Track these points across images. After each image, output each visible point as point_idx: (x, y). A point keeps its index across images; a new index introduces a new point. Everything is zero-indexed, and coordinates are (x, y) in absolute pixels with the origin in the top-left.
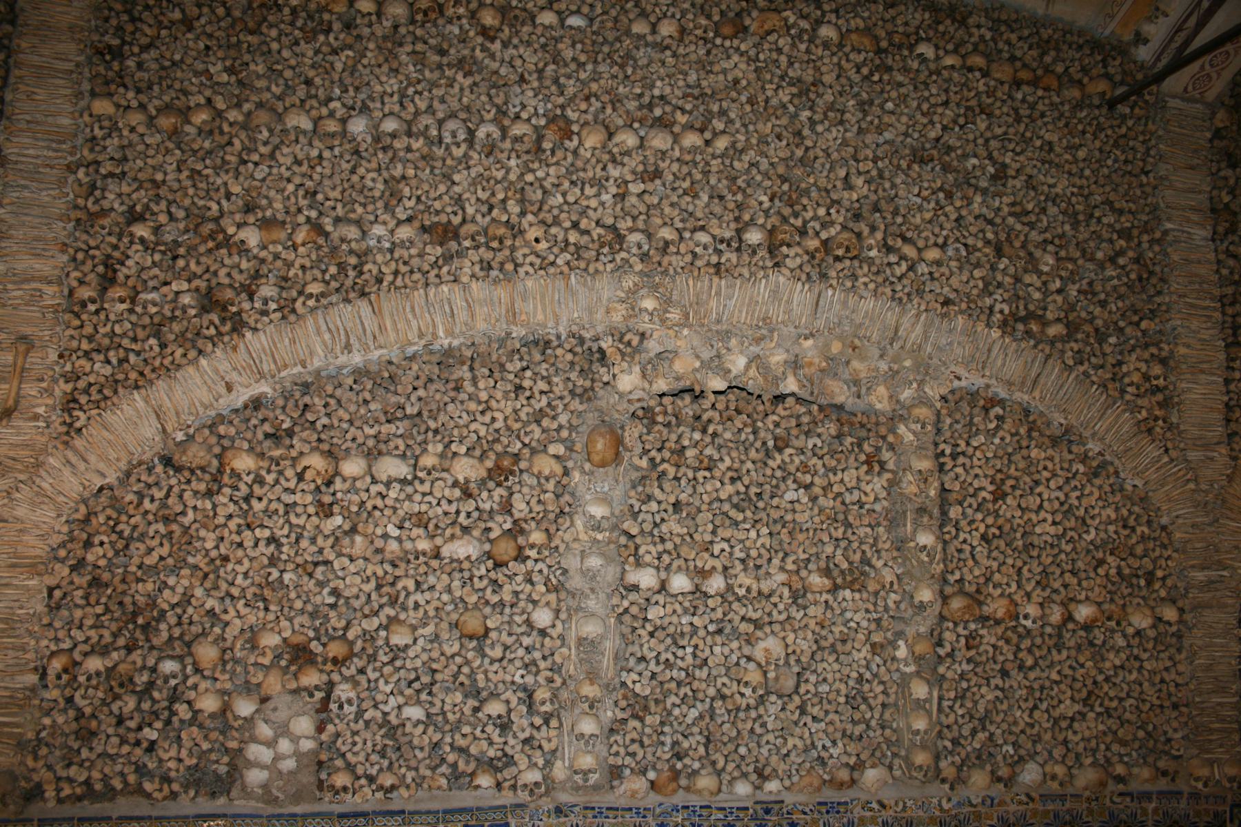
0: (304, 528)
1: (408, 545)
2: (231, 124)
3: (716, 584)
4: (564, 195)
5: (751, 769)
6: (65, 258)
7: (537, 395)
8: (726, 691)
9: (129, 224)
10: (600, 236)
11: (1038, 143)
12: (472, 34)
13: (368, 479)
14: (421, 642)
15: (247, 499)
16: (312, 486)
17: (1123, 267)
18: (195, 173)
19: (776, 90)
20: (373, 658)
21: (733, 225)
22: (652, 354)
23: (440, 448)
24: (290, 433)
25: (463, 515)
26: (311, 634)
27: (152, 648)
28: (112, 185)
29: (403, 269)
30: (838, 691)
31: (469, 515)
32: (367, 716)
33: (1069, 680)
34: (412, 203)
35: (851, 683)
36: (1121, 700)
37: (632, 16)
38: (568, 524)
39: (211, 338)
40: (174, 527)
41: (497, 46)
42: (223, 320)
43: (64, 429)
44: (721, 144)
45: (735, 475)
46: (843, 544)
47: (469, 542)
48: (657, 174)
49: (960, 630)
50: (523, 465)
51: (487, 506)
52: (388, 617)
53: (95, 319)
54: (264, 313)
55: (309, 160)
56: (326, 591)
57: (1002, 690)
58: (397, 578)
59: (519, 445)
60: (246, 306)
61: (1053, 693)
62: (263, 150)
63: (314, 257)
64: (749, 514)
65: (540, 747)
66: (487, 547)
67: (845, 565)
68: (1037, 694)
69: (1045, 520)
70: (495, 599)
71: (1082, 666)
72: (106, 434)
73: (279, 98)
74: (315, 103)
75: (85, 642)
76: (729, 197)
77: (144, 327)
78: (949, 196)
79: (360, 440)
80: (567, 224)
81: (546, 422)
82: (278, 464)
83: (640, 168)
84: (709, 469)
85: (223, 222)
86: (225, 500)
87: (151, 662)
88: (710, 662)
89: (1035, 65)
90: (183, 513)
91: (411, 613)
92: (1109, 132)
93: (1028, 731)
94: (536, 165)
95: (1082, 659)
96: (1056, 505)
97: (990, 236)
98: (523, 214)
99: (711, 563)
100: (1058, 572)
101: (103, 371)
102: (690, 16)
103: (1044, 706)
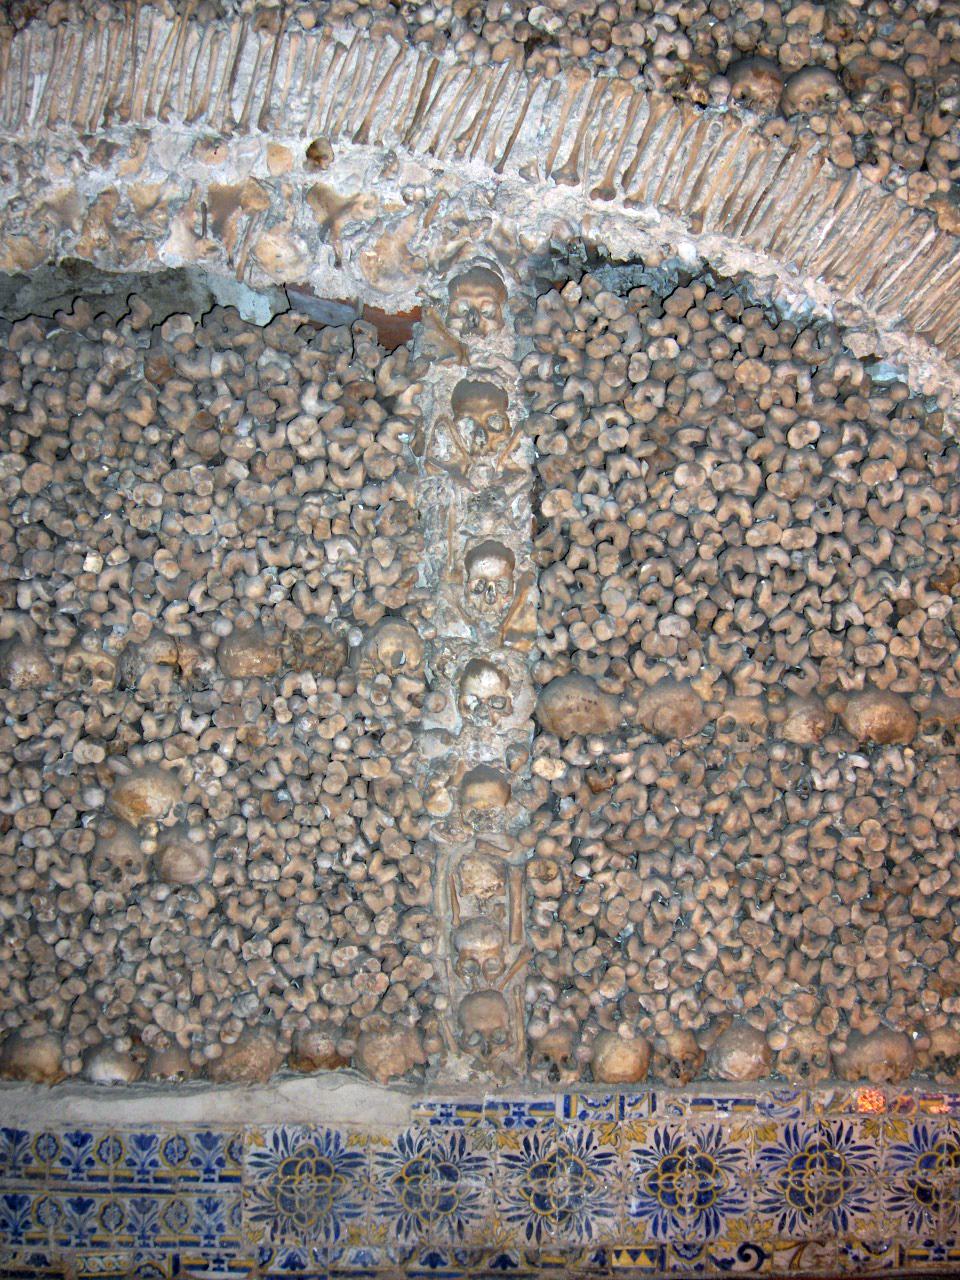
5: (119, 1028)
30: (299, 878)
45: (64, 443)
46: (287, 579)
49: (571, 753)
57: (668, 878)
61: (790, 888)
64: (83, 521)
67: (297, 622)
68: (748, 891)
71: (857, 830)
93: (728, 964)
95: (854, 816)
100: (798, 628)
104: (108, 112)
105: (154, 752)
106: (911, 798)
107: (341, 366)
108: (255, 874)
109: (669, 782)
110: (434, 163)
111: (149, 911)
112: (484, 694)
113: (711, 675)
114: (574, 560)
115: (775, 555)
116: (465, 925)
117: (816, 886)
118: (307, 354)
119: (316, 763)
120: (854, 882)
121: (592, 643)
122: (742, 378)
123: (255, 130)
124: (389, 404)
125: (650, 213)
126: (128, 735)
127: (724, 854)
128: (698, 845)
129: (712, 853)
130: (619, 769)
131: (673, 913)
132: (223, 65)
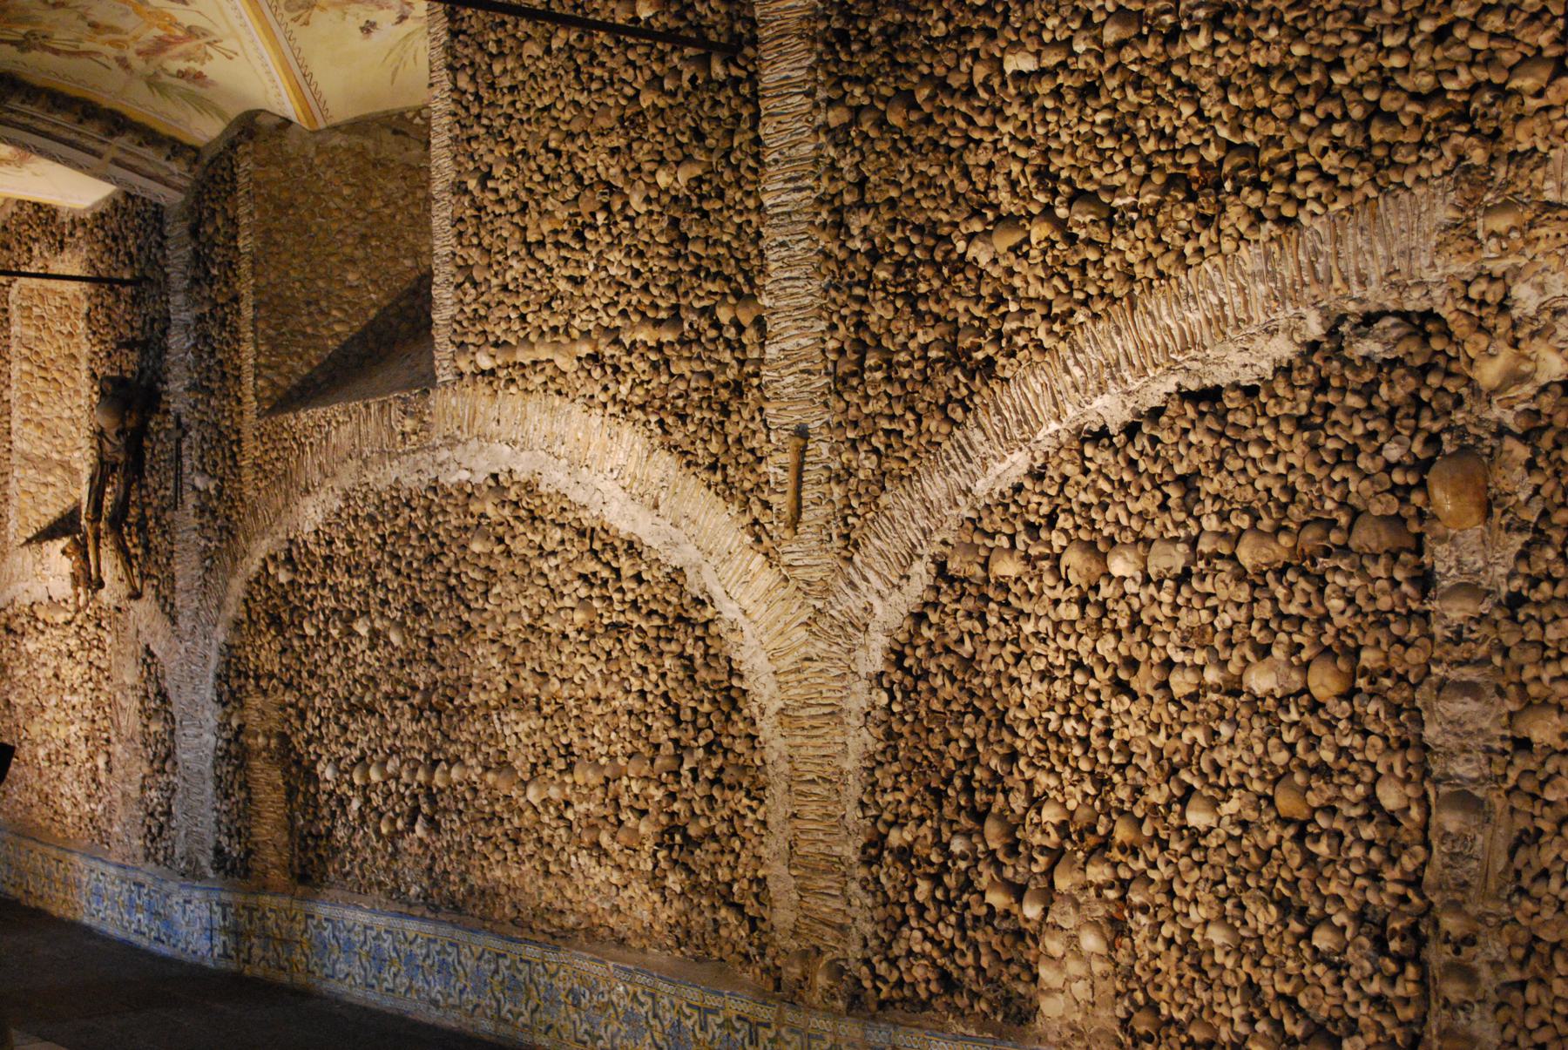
6: (823, 325)
10: (1418, 120)
14: (1226, 820)
16: (1075, 594)
20: (1164, 846)
22: (1531, 311)
24: (1051, 520)
25: (1255, 625)
29: (1156, 251)
31: (1265, 624)
32: (1166, 931)
38: (1414, 632)
39: (961, 402)
42: (971, 375)
50: (1335, 537)
51: (1293, 609)
52: (1189, 790)
54: (1012, 354)
58: (1184, 725)
59: (1329, 505)
60: (990, 350)
63: (1049, 260)
65: (1394, 1012)
66: (1295, 676)
72: (877, 542)
79: (1124, 521)
81: (1363, 462)
90: (961, 641)
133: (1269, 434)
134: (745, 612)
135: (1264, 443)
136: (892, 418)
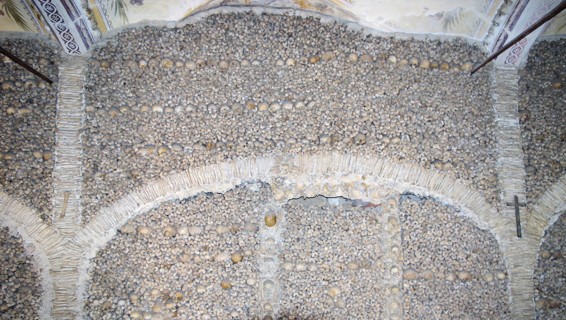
0: (166, 252)
1: (202, 257)
2: (134, 112)
3: (313, 268)
4: (253, 129)
7: (246, 202)
8: (319, 307)
9: (101, 149)
11: (439, 92)
12: (218, 71)
13: (188, 234)
14: (208, 290)
15: (147, 243)
17: (477, 138)
18: (122, 130)
19: (332, 82)
21: (316, 136)
22: (288, 185)
23: (212, 223)
24: (160, 220)
25: (221, 246)
26: (170, 289)
27: (116, 296)
28: (96, 137)
29: (197, 160)
30: (362, 306)
33: (457, 302)
34: (199, 136)
35: (367, 303)
36: (480, 310)
37: (276, 59)
40: (122, 254)
41: (226, 76)
42: (135, 181)
43: (83, 222)
44: (311, 105)
47: (224, 255)
48: (287, 119)
50: (242, 227)
51: (230, 243)
53: (92, 184)
54: (149, 178)
55: (162, 123)
56: (175, 275)
59: (240, 220)
61: (451, 307)
62: (145, 120)
63: (165, 158)
64: (324, 241)
67: (362, 259)
69: (444, 240)
70: (234, 275)
71: (462, 296)
72: (97, 223)
73: (151, 101)
74: (163, 102)
75: (93, 295)
76: (314, 125)
77: (108, 185)
78: (402, 117)
79: (184, 221)
80: (254, 140)
81: (249, 212)
82: (156, 231)
83: (280, 117)
84: (310, 225)
85: (134, 147)
86: (139, 244)
87: (115, 301)
88: (312, 296)
89: (439, 59)
91: (205, 281)
92: (471, 84)
94: (242, 119)
96: (449, 234)
97: (419, 131)
98: (238, 138)
99: (311, 260)
101: (95, 202)
102: (298, 57)
103: (446, 312)
104: (328, 170)
105: (337, 283)
106: (472, 291)
107: (369, 214)
108: (354, 305)
109: (428, 288)
110: (384, 179)
111: (335, 313)
112: (395, 272)
113: (435, 268)
114: (410, 248)
115: (445, 247)
116: (392, 315)
117: (455, 307)
118: (363, 212)
119: (366, 285)
120: (462, 306)
121: (414, 263)
122: (438, 216)
123: (353, 173)
124: (377, 221)
125: (421, 187)
126: (332, 280)
127: (438, 301)
128: (434, 300)
129: (436, 301)
130: (419, 285)
131: (430, 312)
132: (347, 162)
133: (227, 204)
134: (38, 241)
135: (225, 206)
136: (106, 190)
